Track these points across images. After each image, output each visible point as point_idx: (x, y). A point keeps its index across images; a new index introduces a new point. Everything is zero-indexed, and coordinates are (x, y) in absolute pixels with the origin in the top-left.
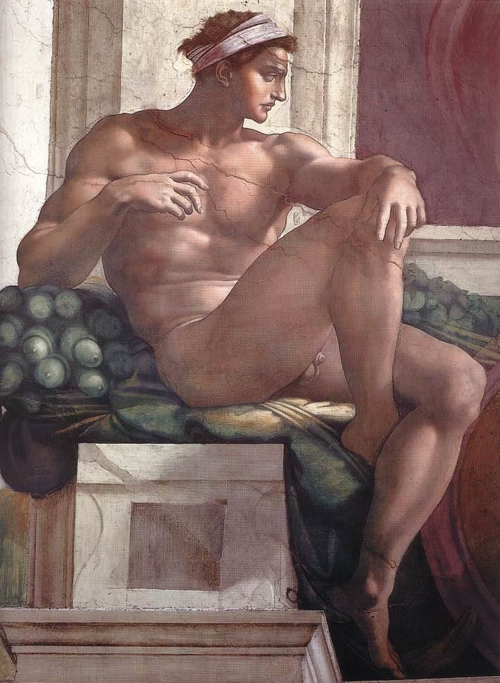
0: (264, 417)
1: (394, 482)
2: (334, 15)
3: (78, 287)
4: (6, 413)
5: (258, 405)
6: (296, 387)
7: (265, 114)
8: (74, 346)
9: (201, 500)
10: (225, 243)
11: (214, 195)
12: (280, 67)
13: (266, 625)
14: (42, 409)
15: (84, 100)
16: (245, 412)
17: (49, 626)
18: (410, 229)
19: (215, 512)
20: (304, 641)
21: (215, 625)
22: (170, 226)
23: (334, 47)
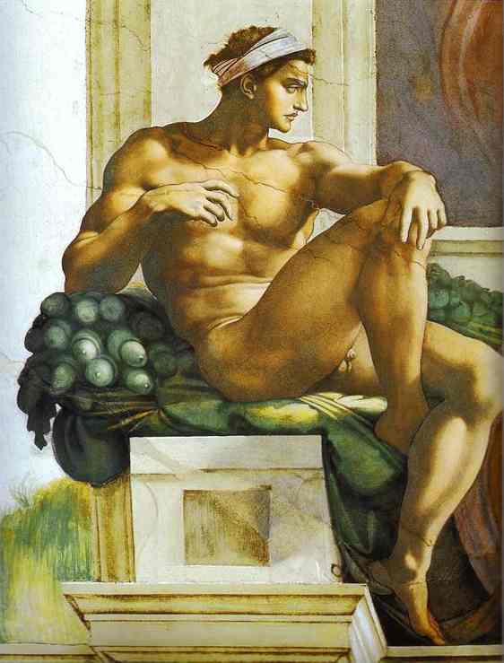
0: (301, 412)
1: (427, 470)
2: (349, 28)
3: (121, 292)
4: (60, 412)
5: (295, 399)
6: (332, 380)
7: (288, 125)
8: (121, 347)
9: (246, 486)
10: (257, 248)
11: (243, 204)
12: (301, 79)
13: (314, 596)
14: (95, 405)
15: (118, 116)
16: (283, 405)
17: (116, 597)
18: (431, 232)
19: (261, 499)
20: (350, 610)
21: (267, 596)
22: (204, 233)
23: (351, 60)
